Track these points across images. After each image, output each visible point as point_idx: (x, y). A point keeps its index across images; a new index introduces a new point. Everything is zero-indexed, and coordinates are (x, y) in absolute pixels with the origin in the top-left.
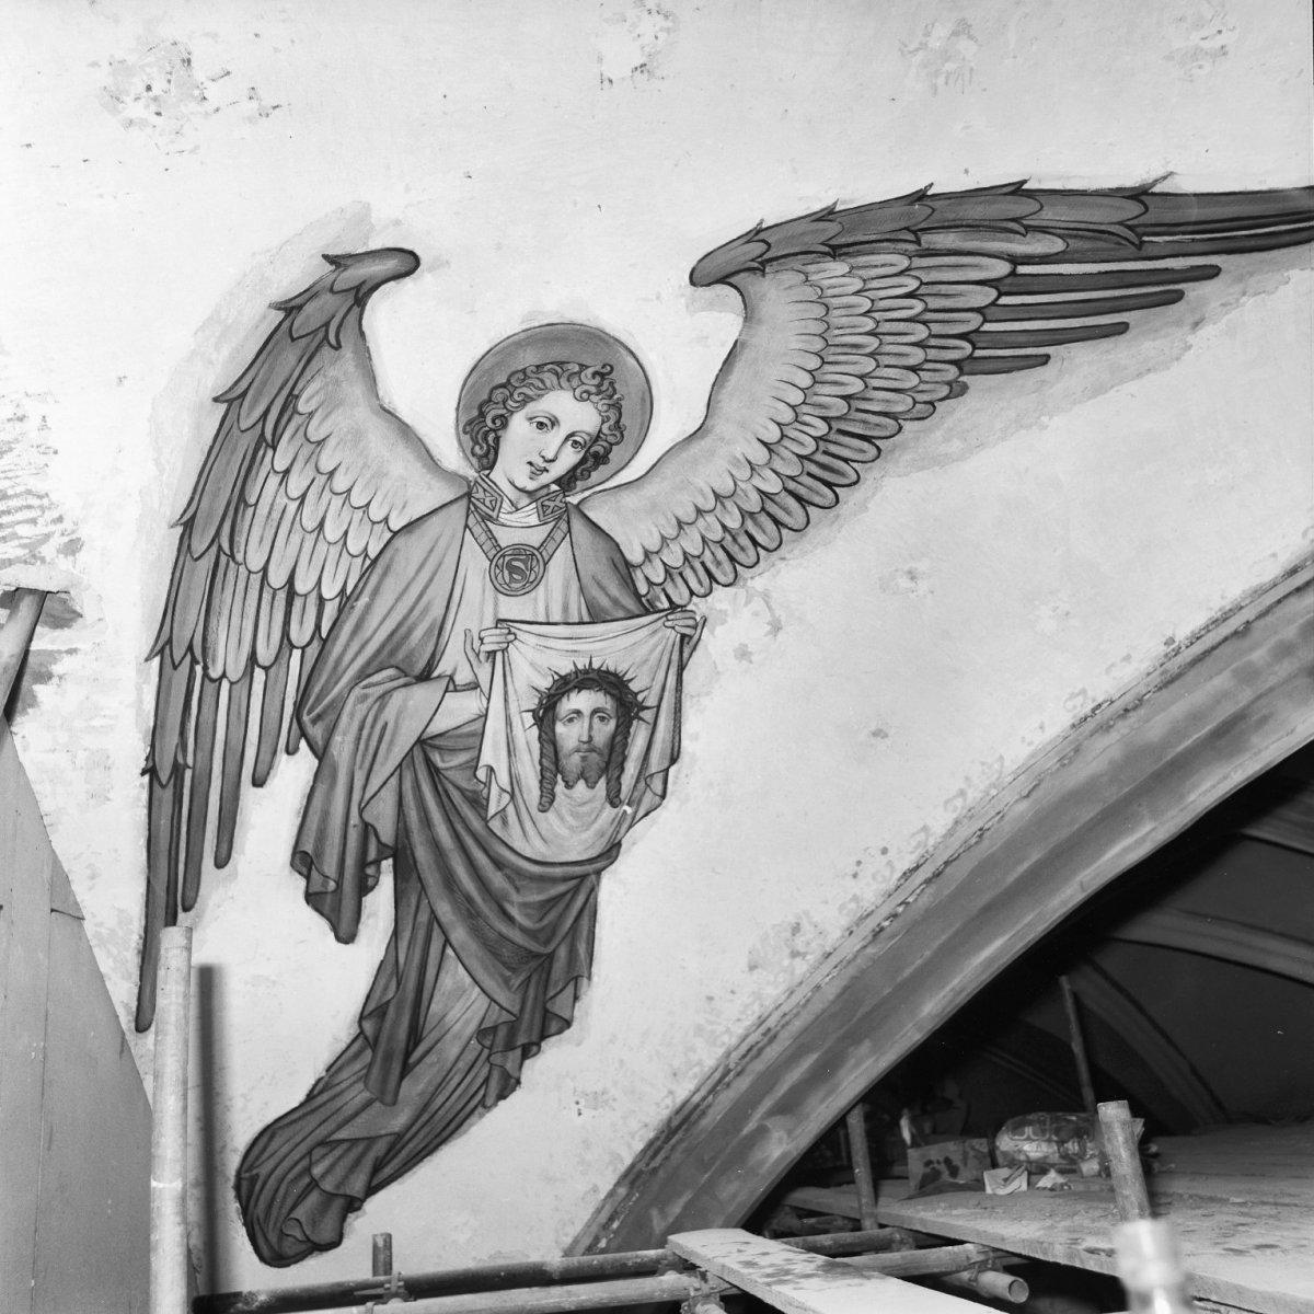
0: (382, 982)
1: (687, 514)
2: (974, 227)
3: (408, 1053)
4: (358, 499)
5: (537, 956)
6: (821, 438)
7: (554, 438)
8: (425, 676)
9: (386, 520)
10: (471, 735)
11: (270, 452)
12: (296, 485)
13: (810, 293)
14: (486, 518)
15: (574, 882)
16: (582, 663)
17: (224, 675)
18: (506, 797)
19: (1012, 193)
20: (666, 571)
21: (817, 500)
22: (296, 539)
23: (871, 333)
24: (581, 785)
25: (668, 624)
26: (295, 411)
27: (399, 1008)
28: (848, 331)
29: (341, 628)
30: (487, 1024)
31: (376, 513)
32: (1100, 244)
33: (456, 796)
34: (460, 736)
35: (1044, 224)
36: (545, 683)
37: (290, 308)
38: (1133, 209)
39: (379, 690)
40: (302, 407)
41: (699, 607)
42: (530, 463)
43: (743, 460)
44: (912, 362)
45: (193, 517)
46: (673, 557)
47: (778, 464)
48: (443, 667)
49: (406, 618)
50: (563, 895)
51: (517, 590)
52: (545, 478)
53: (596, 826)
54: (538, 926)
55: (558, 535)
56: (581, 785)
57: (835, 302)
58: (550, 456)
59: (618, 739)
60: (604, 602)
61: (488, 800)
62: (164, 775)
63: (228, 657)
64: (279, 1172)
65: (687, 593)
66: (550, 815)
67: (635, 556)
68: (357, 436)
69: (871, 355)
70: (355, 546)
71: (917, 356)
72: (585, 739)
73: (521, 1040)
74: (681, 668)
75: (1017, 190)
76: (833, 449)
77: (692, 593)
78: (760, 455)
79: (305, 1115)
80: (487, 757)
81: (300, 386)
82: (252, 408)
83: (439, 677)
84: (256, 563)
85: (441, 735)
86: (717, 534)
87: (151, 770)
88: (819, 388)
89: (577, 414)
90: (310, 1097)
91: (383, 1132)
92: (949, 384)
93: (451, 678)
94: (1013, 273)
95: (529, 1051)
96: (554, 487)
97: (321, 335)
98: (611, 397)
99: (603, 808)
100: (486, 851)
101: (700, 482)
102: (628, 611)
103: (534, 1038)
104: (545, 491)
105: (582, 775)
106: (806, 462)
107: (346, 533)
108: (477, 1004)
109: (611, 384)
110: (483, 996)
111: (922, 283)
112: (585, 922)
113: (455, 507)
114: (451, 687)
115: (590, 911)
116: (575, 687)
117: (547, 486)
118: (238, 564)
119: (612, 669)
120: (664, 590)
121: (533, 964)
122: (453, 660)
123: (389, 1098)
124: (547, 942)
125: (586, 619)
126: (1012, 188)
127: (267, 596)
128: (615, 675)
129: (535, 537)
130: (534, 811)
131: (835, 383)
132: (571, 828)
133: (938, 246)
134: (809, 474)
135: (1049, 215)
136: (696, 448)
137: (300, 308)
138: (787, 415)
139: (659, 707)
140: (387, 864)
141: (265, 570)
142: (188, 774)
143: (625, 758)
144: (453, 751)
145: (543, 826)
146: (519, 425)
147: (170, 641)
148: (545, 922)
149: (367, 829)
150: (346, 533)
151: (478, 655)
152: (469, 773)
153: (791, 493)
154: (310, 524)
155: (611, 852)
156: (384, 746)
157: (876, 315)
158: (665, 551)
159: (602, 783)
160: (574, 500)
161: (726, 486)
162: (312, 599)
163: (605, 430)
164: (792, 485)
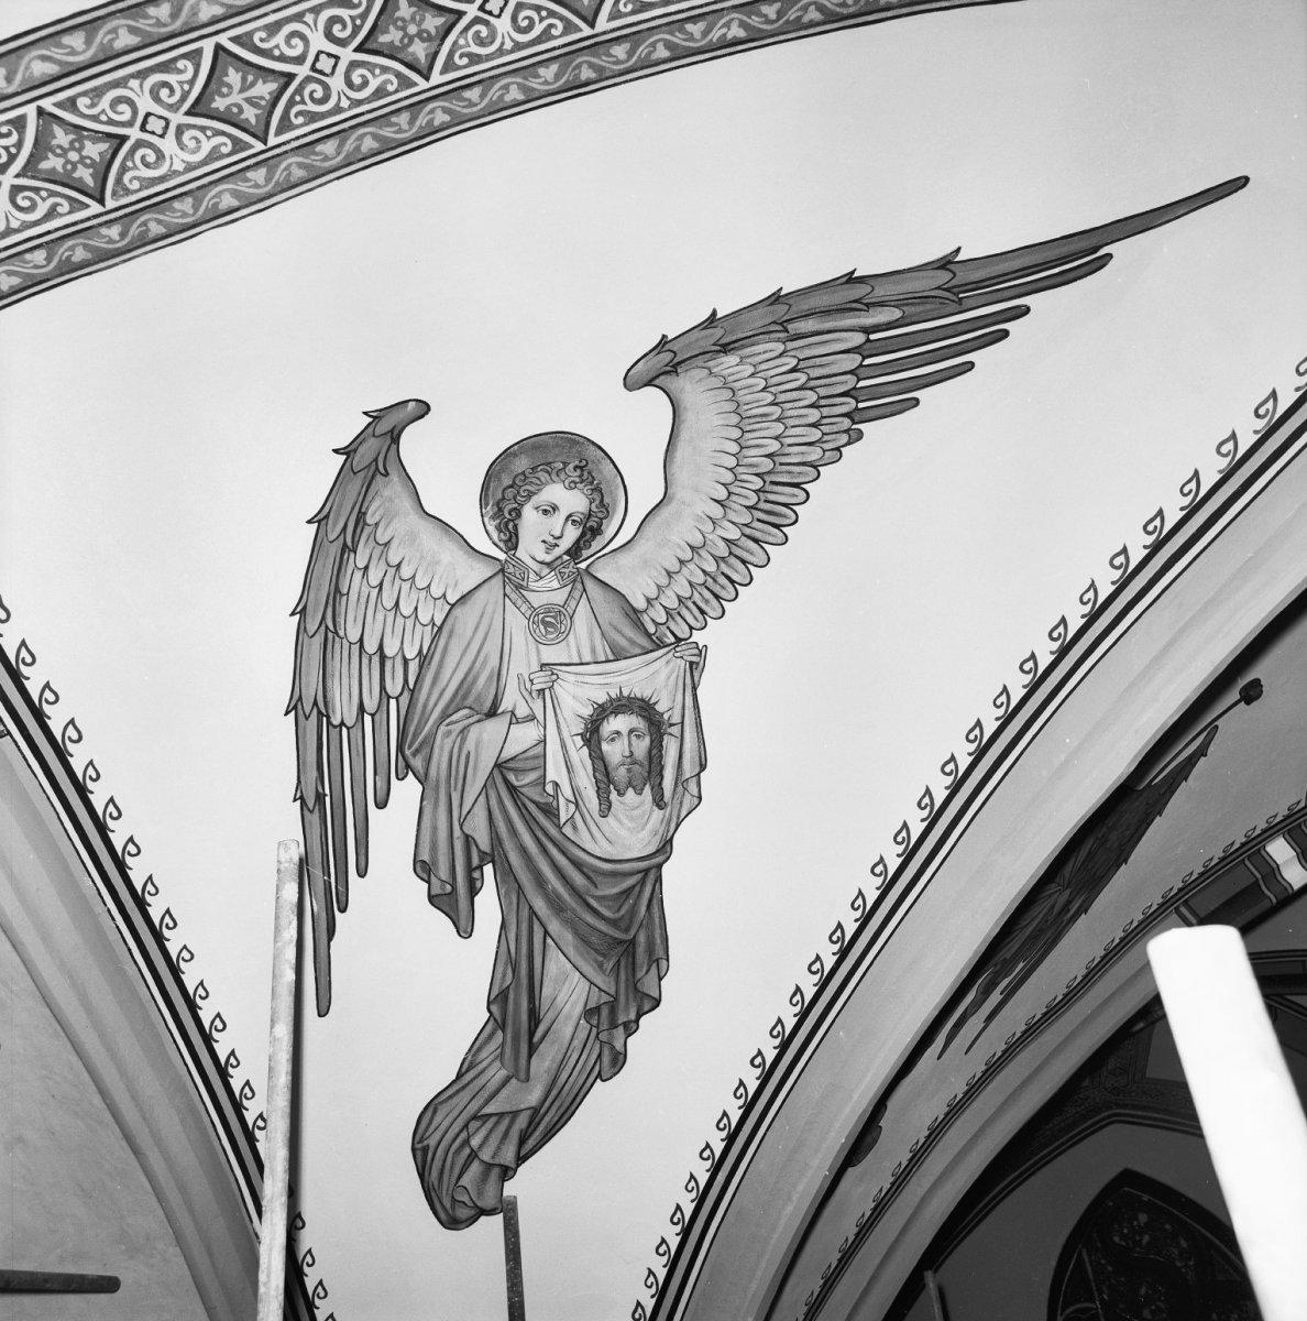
0: (500, 969)
2: (826, 312)
3: (531, 1034)
4: (421, 582)
5: (621, 942)
6: (759, 490)
7: (559, 518)
8: (492, 713)
9: (444, 595)
10: (535, 757)
11: (352, 555)
12: (374, 576)
13: (718, 382)
14: (519, 587)
15: (640, 876)
16: (614, 693)
17: (342, 723)
18: (572, 807)
19: (847, 282)
20: (667, 613)
21: (771, 539)
22: (380, 616)
23: (773, 404)
26: (365, 524)
27: (517, 995)
29: (423, 680)
30: (592, 1004)
31: (436, 591)
32: (928, 307)
34: (527, 759)
35: (879, 300)
36: (587, 711)
37: (348, 452)
38: (944, 276)
39: (459, 727)
40: (370, 520)
41: (697, 637)
42: (544, 541)
43: (704, 517)
44: (812, 420)
45: (305, 608)
47: (732, 516)
48: (505, 705)
49: (470, 669)
50: (634, 886)
51: (553, 640)
52: (558, 552)
53: (649, 827)
54: (617, 916)
55: (577, 594)
58: (558, 534)
59: (654, 752)
60: (623, 642)
61: (558, 809)
62: (311, 803)
63: (343, 710)
66: (610, 819)
67: (640, 604)
68: (412, 537)
69: (778, 420)
70: (424, 617)
71: (814, 416)
72: (627, 754)
73: (622, 1019)
74: (694, 688)
75: (850, 279)
76: (772, 497)
77: (691, 628)
78: (717, 511)
79: (458, 1092)
81: (365, 505)
82: (334, 526)
83: (503, 713)
84: (354, 636)
85: (512, 759)
86: (700, 578)
88: (746, 452)
89: (571, 500)
90: (459, 1076)
91: (522, 1106)
92: (846, 431)
93: (513, 713)
94: (868, 340)
95: (631, 1028)
96: (566, 558)
97: (373, 468)
98: (592, 483)
99: (652, 811)
100: (564, 853)
101: (675, 538)
102: (643, 648)
103: (632, 1016)
104: (559, 562)
105: (630, 784)
106: (753, 511)
107: (416, 608)
109: (589, 473)
110: (583, 979)
111: (799, 360)
112: (655, 910)
113: (494, 581)
114: (514, 720)
115: (656, 900)
116: (612, 713)
117: (560, 557)
118: (342, 638)
119: (639, 696)
120: (668, 628)
121: (620, 949)
123: (522, 1075)
124: (627, 930)
125: (611, 657)
126: (844, 279)
127: (365, 661)
128: (642, 700)
129: (559, 597)
131: (758, 446)
133: (803, 331)
134: (759, 520)
135: (881, 291)
136: (665, 512)
137: (355, 451)
139: (682, 723)
140: (488, 869)
141: (361, 640)
142: (328, 799)
143: (662, 768)
144: (524, 771)
145: (605, 828)
146: (529, 512)
147: (300, 698)
148: (623, 912)
149: (468, 840)
150: (416, 608)
151: (531, 693)
152: (540, 788)
153: (748, 537)
154: (389, 604)
155: (666, 847)
156: (470, 770)
157: (772, 389)
158: (662, 596)
159: (647, 789)
160: (583, 566)
161: (697, 540)
162: (399, 661)
163: (594, 508)
164: (748, 531)
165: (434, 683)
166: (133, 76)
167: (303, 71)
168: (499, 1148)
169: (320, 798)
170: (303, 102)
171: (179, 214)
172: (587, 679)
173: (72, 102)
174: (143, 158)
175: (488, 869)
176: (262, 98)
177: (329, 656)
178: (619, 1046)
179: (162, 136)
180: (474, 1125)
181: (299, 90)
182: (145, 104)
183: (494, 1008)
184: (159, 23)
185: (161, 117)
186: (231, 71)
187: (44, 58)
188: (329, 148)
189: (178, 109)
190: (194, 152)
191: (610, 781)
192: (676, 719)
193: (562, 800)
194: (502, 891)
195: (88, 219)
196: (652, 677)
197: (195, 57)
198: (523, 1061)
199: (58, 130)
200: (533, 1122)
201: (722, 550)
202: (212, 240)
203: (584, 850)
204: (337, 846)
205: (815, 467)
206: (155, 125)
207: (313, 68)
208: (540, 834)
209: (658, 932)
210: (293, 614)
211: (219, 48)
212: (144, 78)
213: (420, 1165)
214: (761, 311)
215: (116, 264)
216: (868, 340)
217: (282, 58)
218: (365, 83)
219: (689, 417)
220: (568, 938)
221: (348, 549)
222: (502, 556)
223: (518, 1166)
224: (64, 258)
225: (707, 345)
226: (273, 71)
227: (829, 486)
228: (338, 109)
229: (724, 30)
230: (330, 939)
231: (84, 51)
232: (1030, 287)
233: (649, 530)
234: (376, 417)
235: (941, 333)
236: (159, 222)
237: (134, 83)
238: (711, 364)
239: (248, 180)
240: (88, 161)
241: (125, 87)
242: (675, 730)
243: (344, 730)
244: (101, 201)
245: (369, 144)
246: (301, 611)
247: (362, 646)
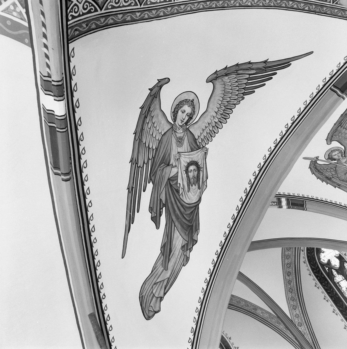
1: (204, 128)
5: (190, 226)
8: (168, 165)
10: (176, 177)
13: (223, 83)
15: (194, 208)
16: (191, 160)
17: (140, 166)
18: (182, 190)
19: (249, 63)
20: (202, 140)
21: (224, 122)
23: (231, 89)
24: (194, 185)
25: (203, 150)
26: (150, 111)
27: (167, 244)
28: (228, 89)
32: (261, 71)
33: (174, 190)
34: (174, 177)
35: (252, 68)
36: (186, 165)
38: (265, 64)
39: (162, 168)
40: (151, 110)
41: (207, 146)
44: (237, 94)
46: (202, 137)
49: (165, 153)
50: (193, 211)
52: (183, 123)
54: (190, 219)
55: (185, 134)
56: (194, 185)
57: (226, 84)
58: (184, 118)
59: (198, 175)
60: (193, 147)
61: (179, 191)
62: (130, 190)
63: (140, 163)
64: (147, 294)
65: (205, 144)
66: (190, 193)
67: (197, 137)
68: (158, 115)
69: (231, 93)
70: (157, 139)
72: (193, 176)
74: (206, 159)
75: (250, 63)
76: (226, 112)
77: (206, 144)
78: (215, 114)
79: (151, 277)
80: (179, 182)
81: (151, 105)
82: (144, 110)
83: (171, 165)
84: (144, 142)
85: (172, 177)
86: (209, 131)
87: (128, 189)
88: (224, 100)
91: (166, 278)
92: (242, 97)
94: (249, 77)
96: (185, 125)
100: (180, 203)
102: (196, 148)
103: (191, 247)
104: (183, 126)
105: (194, 183)
108: (181, 240)
109: (193, 103)
112: (197, 216)
118: (142, 142)
119: (195, 161)
120: (201, 144)
121: (190, 228)
122: (172, 161)
123: (166, 269)
124: (191, 223)
128: (196, 162)
129: (182, 135)
130: (187, 192)
131: (226, 99)
132: (193, 195)
133: (240, 73)
134: (222, 117)
135: (254, 66)
138: (219, 106)
139: (203, 167)
140: (164, 208)
141: (145, 143)
142: (134, 189)
144: (174, 180)
145: (188, 195)
146: (180, 112)
148: (191, 218)
149: (161, 200)
152: (176, 185)
154: (151, 134)
156: (163, 181)
157: (231, 86)
160: (187, 127)
162: (152, 149)
164: (220, 120)
165: (158, 156)
168: (160, 292)
169: (132, 188)
172: (186, 156)
175: (164, 208)
177: (139, 147)
178: (188, 256)
180: (154, 286)
183: (162, 249)
191: (190, 183)
192: (202, 167)
193: (180, 188)
194: (166, 215)
195: (136, 9)
196: (197, 156)
198: (167, 265)
200: (168, 283)
201: (214, 125)
202: (155, 23)
203: (184, 202)
204: (134, 202)
205: (235, 105)
208: (175, 198)
209: (197, 222)
210: (134, 134)
213: (141, 302)
214: (234, 67)
215: (134, 24)
216: (249, 77)
219: (216, 91)
220: (179, 226)
221: (146, 117)
222: (173, 123)
223: (164, 296)
225: (223, 74)
227: (237, 110)
229: (248, 3)
230: (128, 233)
232: (276, 69)
233: (202, 118)
234: (159, 81)
235: (261, 77)
238: (223, 78)
242: (202, 169)
243: (140, 168)
246: (135, 133)
247: (145, 145)
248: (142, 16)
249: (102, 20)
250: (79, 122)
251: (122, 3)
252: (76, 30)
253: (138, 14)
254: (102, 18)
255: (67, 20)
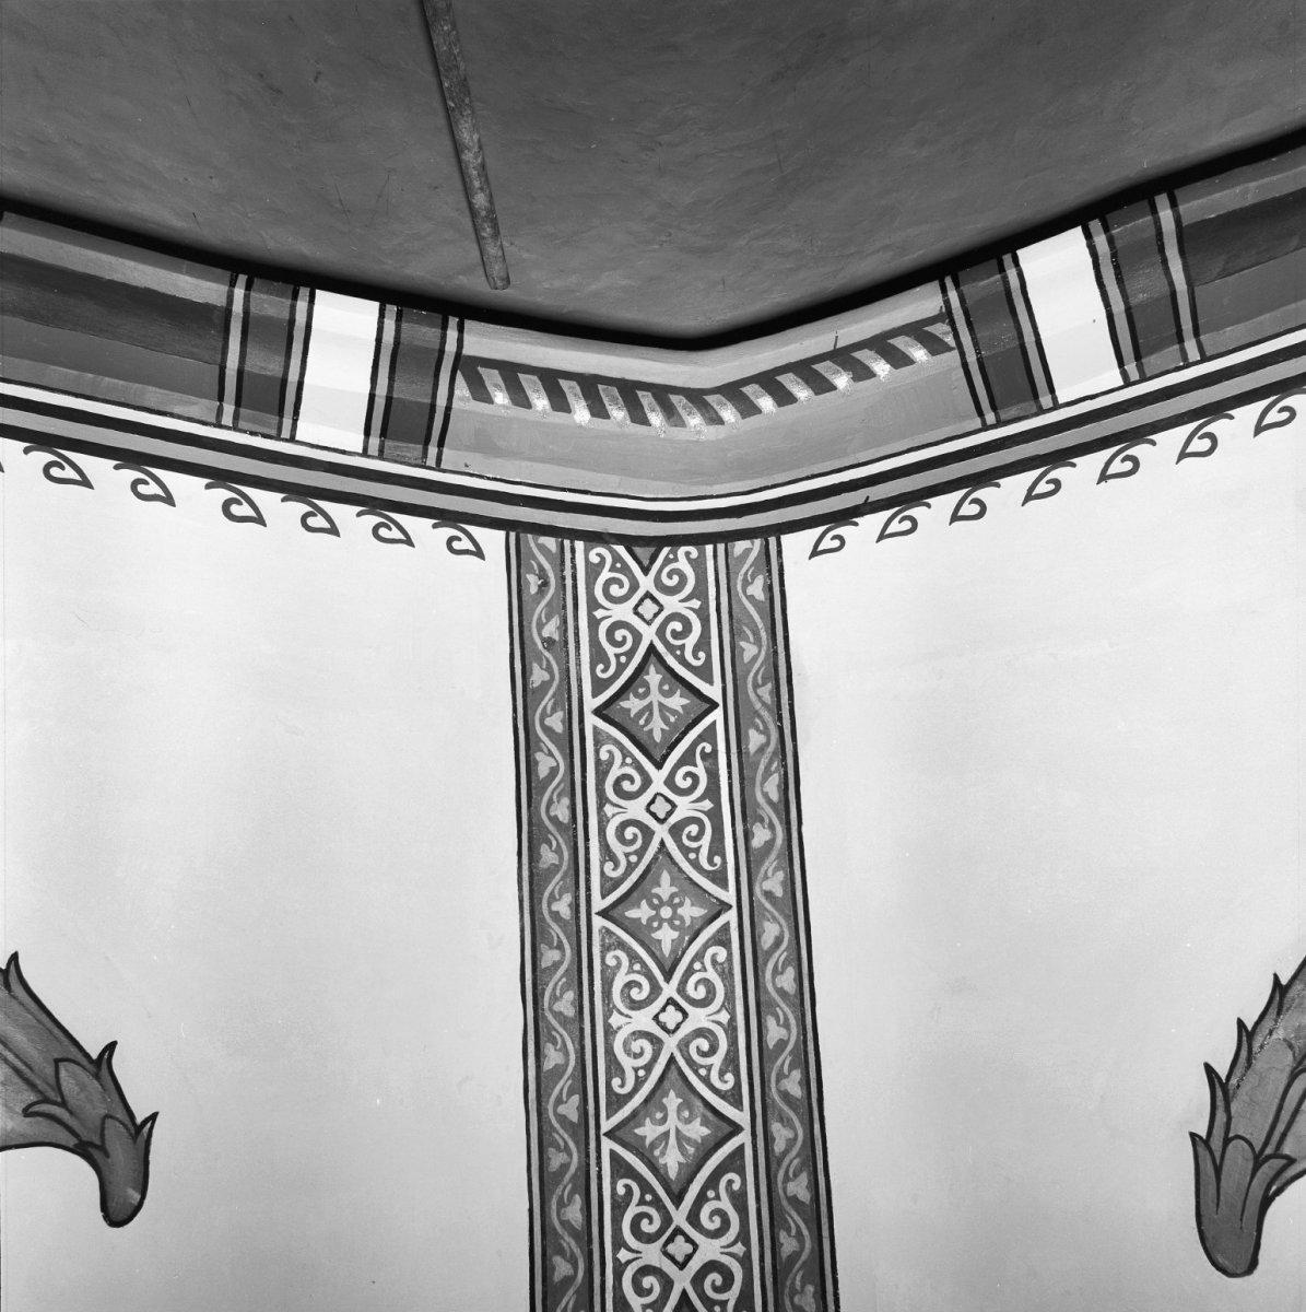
97: (52, 1095)
137: (97, 1077)
166: (733, 1019)
167: (679, 1217)
170: (642, 1202)
171: (558, 994)
173: (726, 944)
174: (639, 985)
176: (663, 1153)
179: (656, 1018)
181: (657, 1203)
182: (699, 1018)
184: (781, 1076)
185: (678, 1026)
186: (705, 1131)
187: (778, 942)
188: (574, 1213)
189: (681, 1051)
190: (626, 1044)
195: (588, 889)
197: (734, 1097)
199: (699, 912)
202: (511, 1017)
206: (671, 1017)
207: (679, 1231)
211: (736, 1129)
212: (726, 1031)
217: (701, 1199)
218: (641, 1291)
224: (550, 836)
226: (690, 1180)
228: (619, 1243)
231: (774, 984)
234: (140, 1133)
236: (556, 965)
237: (724, 1017)
239: (570, 1094)
240: (655, 924)
241: (723, 1005)
244: (604, 914)
245: (562, 1268)
248: (556, 929)
249: (556, 722)
250: (152, 489)
251: (617, 810)
252: (545, 584)
253: (563, 907)
254: (563, 722)
255: (593, 538)
